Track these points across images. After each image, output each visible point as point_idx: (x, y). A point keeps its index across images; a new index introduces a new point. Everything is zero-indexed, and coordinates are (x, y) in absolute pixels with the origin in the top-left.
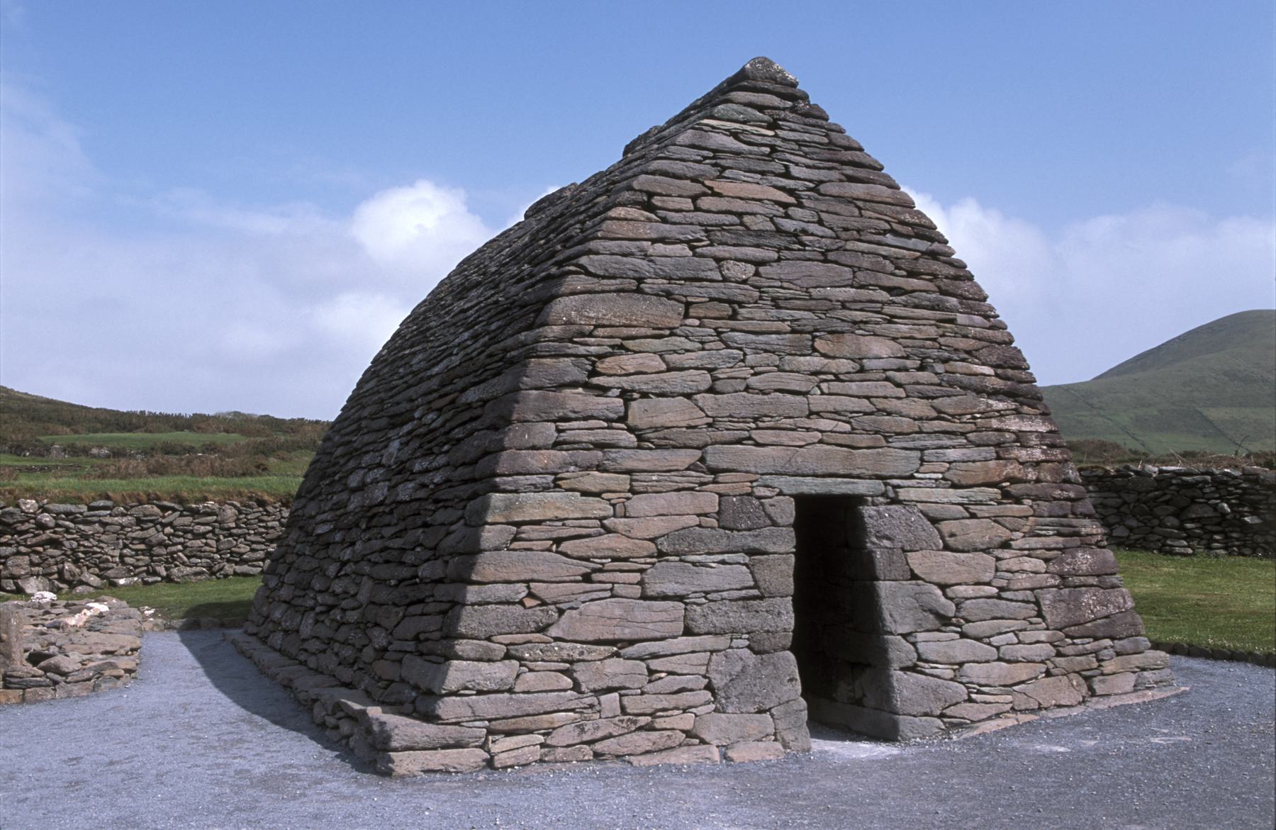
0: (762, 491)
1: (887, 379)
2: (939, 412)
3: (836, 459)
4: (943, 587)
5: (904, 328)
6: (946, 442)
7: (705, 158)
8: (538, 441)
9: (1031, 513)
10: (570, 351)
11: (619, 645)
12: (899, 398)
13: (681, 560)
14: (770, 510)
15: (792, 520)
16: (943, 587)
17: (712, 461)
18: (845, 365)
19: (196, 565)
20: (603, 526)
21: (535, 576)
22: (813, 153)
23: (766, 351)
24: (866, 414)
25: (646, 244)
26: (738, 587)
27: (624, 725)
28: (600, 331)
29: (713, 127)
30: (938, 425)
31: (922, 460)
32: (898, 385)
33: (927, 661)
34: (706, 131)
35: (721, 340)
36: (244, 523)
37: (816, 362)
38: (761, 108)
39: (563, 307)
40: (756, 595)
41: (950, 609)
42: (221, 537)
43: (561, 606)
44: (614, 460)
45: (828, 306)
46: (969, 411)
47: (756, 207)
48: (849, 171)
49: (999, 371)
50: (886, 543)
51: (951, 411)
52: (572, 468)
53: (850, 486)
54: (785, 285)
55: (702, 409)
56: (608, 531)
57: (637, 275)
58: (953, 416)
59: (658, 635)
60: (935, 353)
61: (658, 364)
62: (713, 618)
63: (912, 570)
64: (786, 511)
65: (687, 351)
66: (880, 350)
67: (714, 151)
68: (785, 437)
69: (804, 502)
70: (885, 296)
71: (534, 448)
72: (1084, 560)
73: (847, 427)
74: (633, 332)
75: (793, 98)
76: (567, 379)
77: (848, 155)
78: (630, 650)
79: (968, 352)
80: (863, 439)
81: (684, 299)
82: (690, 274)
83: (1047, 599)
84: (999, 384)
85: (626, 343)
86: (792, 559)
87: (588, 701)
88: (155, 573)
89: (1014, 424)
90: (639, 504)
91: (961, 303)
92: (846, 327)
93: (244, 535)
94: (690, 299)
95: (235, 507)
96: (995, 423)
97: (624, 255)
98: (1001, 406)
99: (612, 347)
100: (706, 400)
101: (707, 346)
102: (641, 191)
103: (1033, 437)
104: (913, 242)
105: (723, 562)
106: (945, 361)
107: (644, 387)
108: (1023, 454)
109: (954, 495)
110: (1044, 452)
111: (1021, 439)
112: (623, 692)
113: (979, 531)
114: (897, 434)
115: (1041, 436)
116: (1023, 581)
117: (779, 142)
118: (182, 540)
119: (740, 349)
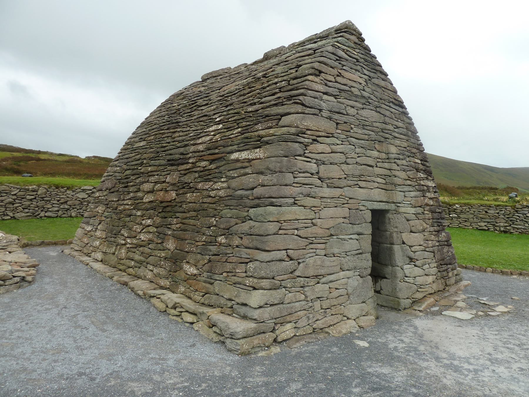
2: (409, 177)
7: (337, 60)
9: (432, 218)
10: (299, 140)
12: (398, 170)
13: (337, 238)
14: (365, 216)
15: (370, 220)
16: (410, 247)
19: (27, 213)
20: (312, 223)
21: (290, 247)
22: (369, 65)
23: (362, 147)
24: (390, 176)
25: (322, 94)
26: (356, 249)
27: (323, 314)
28: (309, 132)
29: (339, 47)
30: (409, 182)
31: (405, 196)
32: (398, 165)
33: (407, 277)
34: (336, 48)
35: (348, 141)
36: (50, 196)
41: (412, 255)
42: (39, 201)
43: (300, 261)
44: (315, 192)
50: (396, 230)
52: (301, 195)
54: (366, 119)
55: (343, 171)
56: (314, 225)
57: (319, 108)
59: (332, 272)
62: (349, 263)
63: (403, 240)
64: (368, 216)
65: (338, 144)
67: (340, 57)
71: (286, 185)
73: (384, 181)
74: (320, 134)
78: (324, 280)
81: (336, 121)
82: (337, 110)
85: (318, 139)
86: (371, 237)
87: (310, 304)
88: (8, 215)
93: (50, 201)
94: (338, 121)
95: (45, 188)
97: (315, 98)
99: (314, 140)
100: (344, 167)
101: (343, 143)
102: (317, 70)
105: (351, 239)
109: (413, 210)
112: (321, 299)
114: (399, 185)
118: (21, 202)
119: (354, 145)
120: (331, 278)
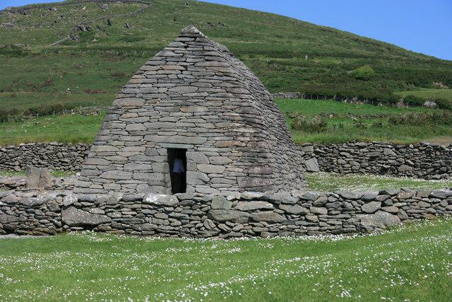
0: (156, 147)
3: (181, 139)
4: (208, 174)
6: (216, 135)
11: (116, 180)
14: (159, 152)
16: (208, 174)
18: (188, 114)
30: (214, 131)
37: (180, 113)
38: (184, 42)
40: (151, 171)
47: (173, 72)
48: (207, 58)
60: (219, 110)
61: (136, 115)
66: (201, 110)
69: (169, 150)
72: (257, 170)
75: (195, 38)
80: (190, 134)
83: (240, 179)
89: (242, 130)
90: (125, 149)
92: (191, 104)
96: (235, 130)
98: (238, 125)
104: (221, 78)
106: (223, 112)
108: (242, 139)
109: (217, 150)
111: (243, 135)
113: (220, 160)
116: (233, 174)
117: (186, 52)
120: (123, 182)
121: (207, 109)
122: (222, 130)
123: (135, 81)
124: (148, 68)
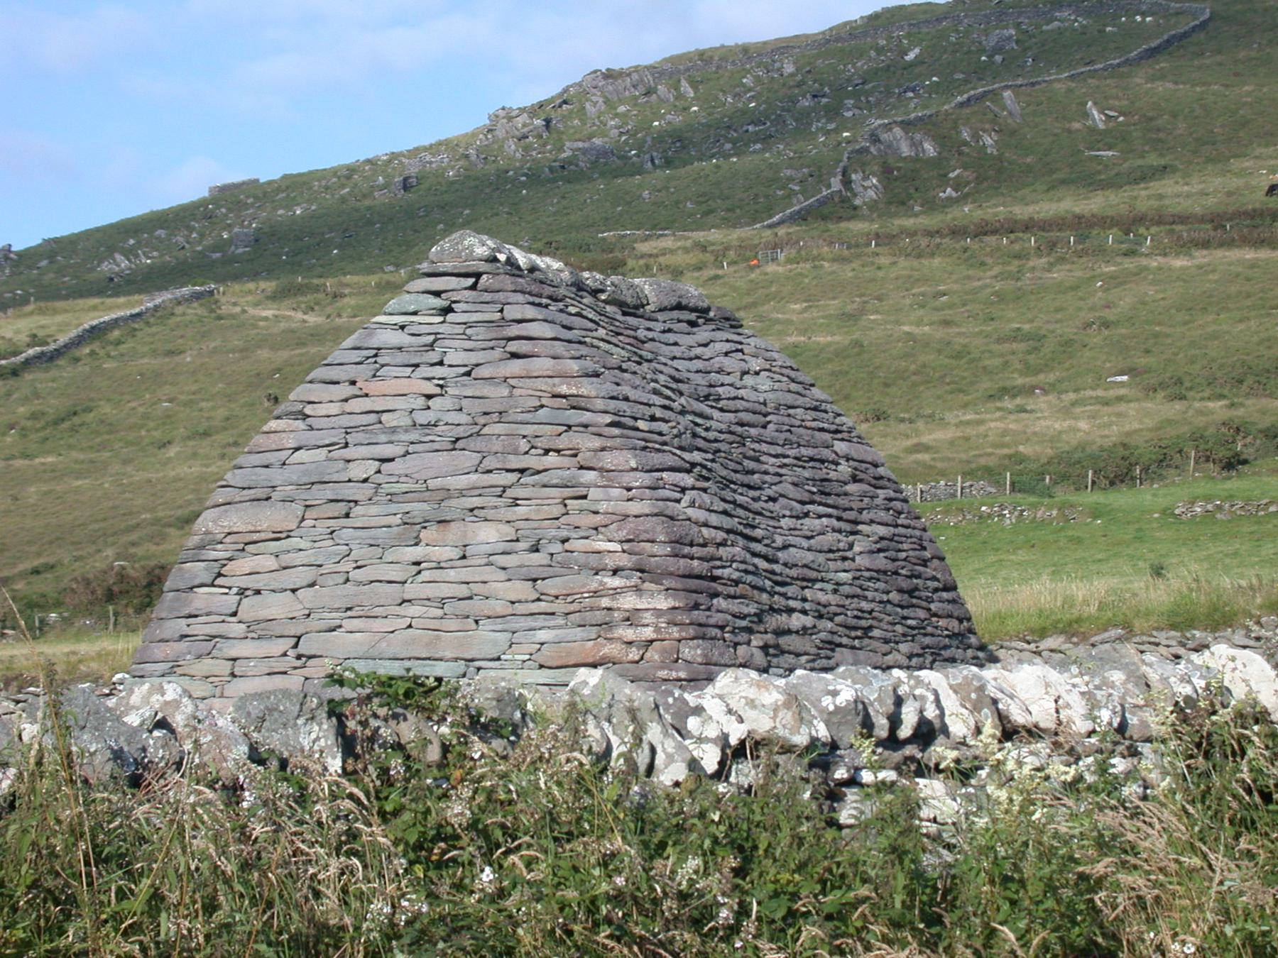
1: (490, 564)
3: (416, 642)
5: (521, 511)
8: (167, 635)
17: (302, 649)
28: (228, 539)
30: (535, 607)
38: (437, 294)
39: (208, 522)
45: (447, 493)
46: (577, 590)
48: (514, 346)
49: (626, 546)
51: (553, 592)
53: (428, 669)
54: (402, 479)
58: (557, 597)
60: (553, 532)
61: (272, 563)
66: (488, 535)
68: (377, 625)
70: (513, 477)
71: (161, 641)
73: (439, 612)
74: (255, 537)
76: (197, 582)
77: (515, 330)
79: (596, 529)
80: (453, 624)
84: (624, 560)
89: (629, 602)
91: (603, 477)
96: (605, 602)
103: (648, 615)
106: (564, 541)
107: (257, 586)
108: (629, 634)
110: (657, 629)
111: (631, 618)
115: (658, 612)
117: (442, 329)
121: (509, 532)
122: (559, 606)
123: (272, 441)
124: (317, 391)
